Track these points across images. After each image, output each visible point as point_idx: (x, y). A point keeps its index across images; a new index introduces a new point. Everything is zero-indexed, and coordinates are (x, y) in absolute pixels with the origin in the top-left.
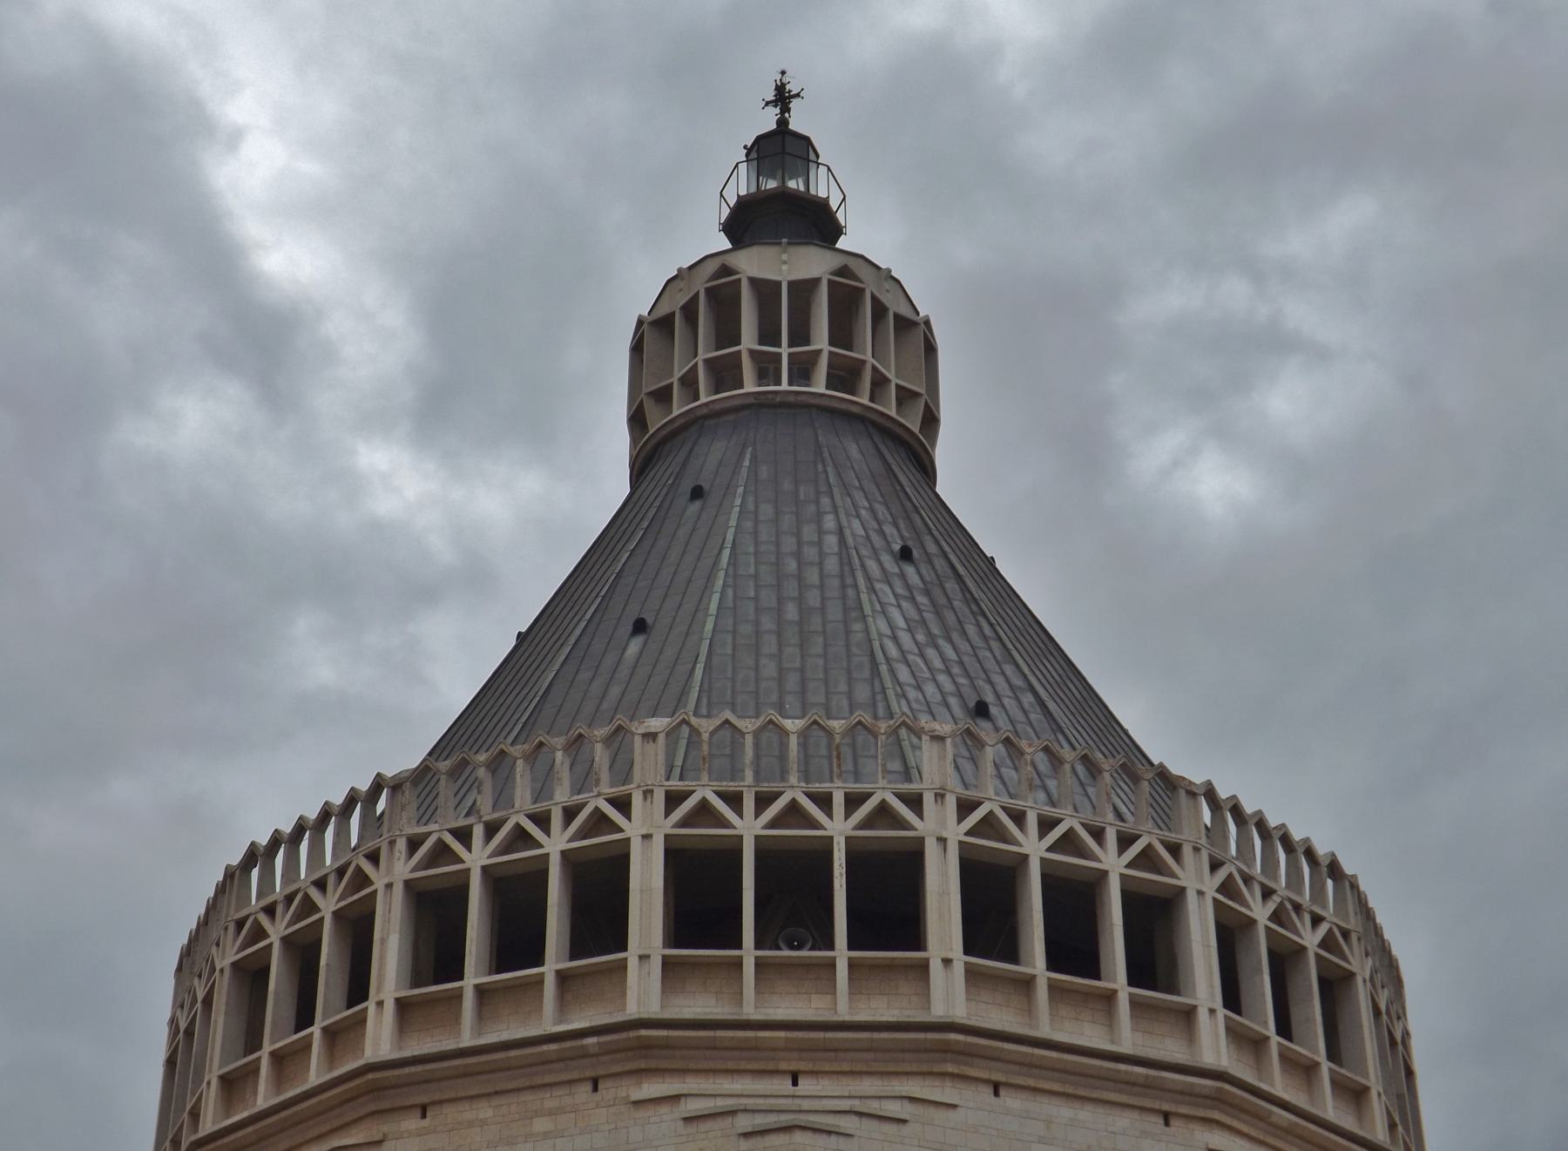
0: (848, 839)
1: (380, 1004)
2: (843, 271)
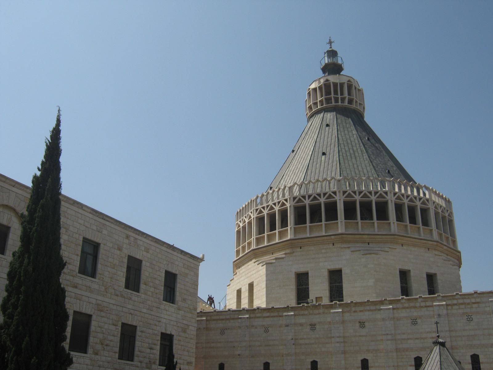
0: (375, 200)
2: (349, 81)
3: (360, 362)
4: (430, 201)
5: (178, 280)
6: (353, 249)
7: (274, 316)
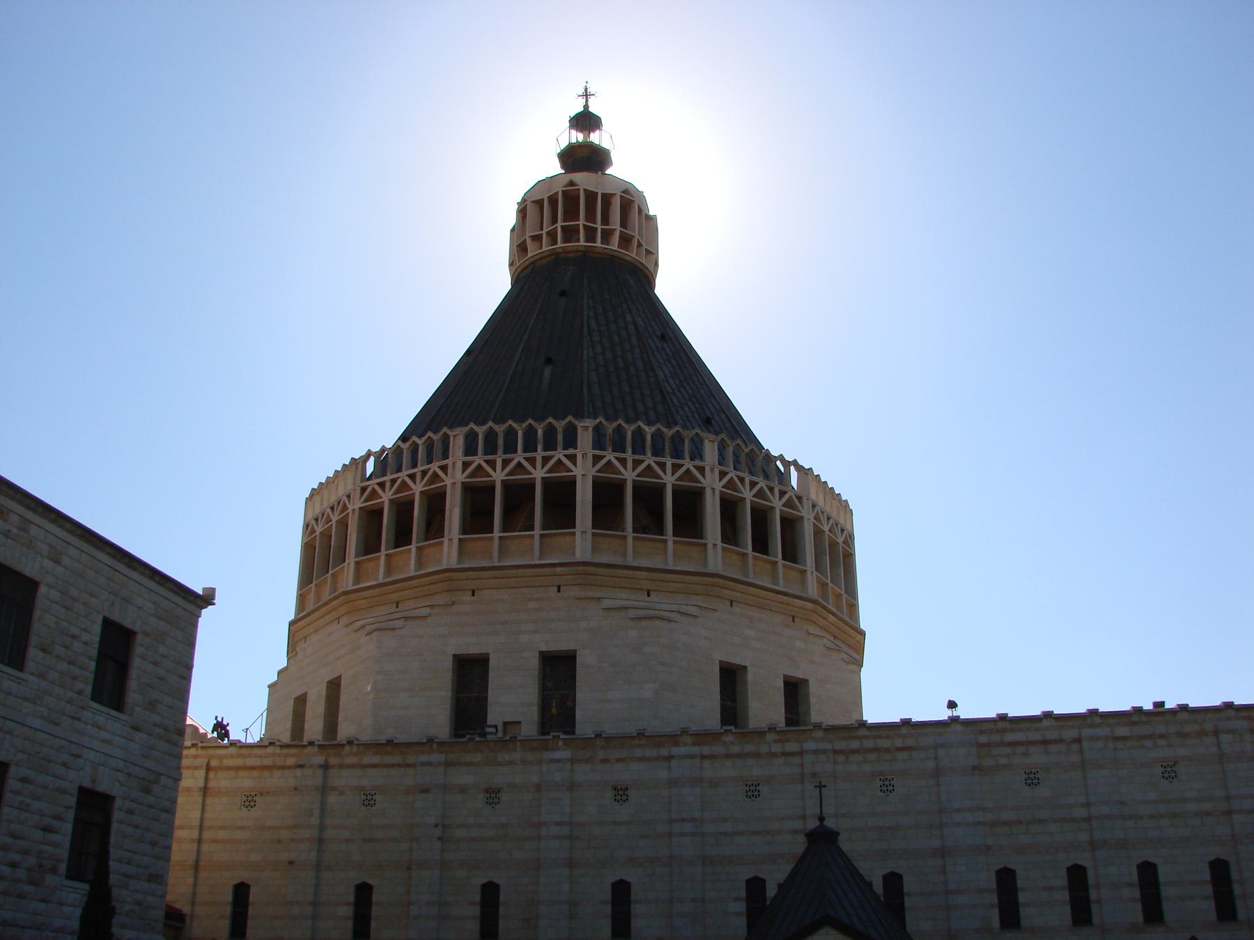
1: (450, 540)
3: (609, 889)
4: (804, 499)
5: (138, 650)
6: (607, 603)
7: (393, 766)
